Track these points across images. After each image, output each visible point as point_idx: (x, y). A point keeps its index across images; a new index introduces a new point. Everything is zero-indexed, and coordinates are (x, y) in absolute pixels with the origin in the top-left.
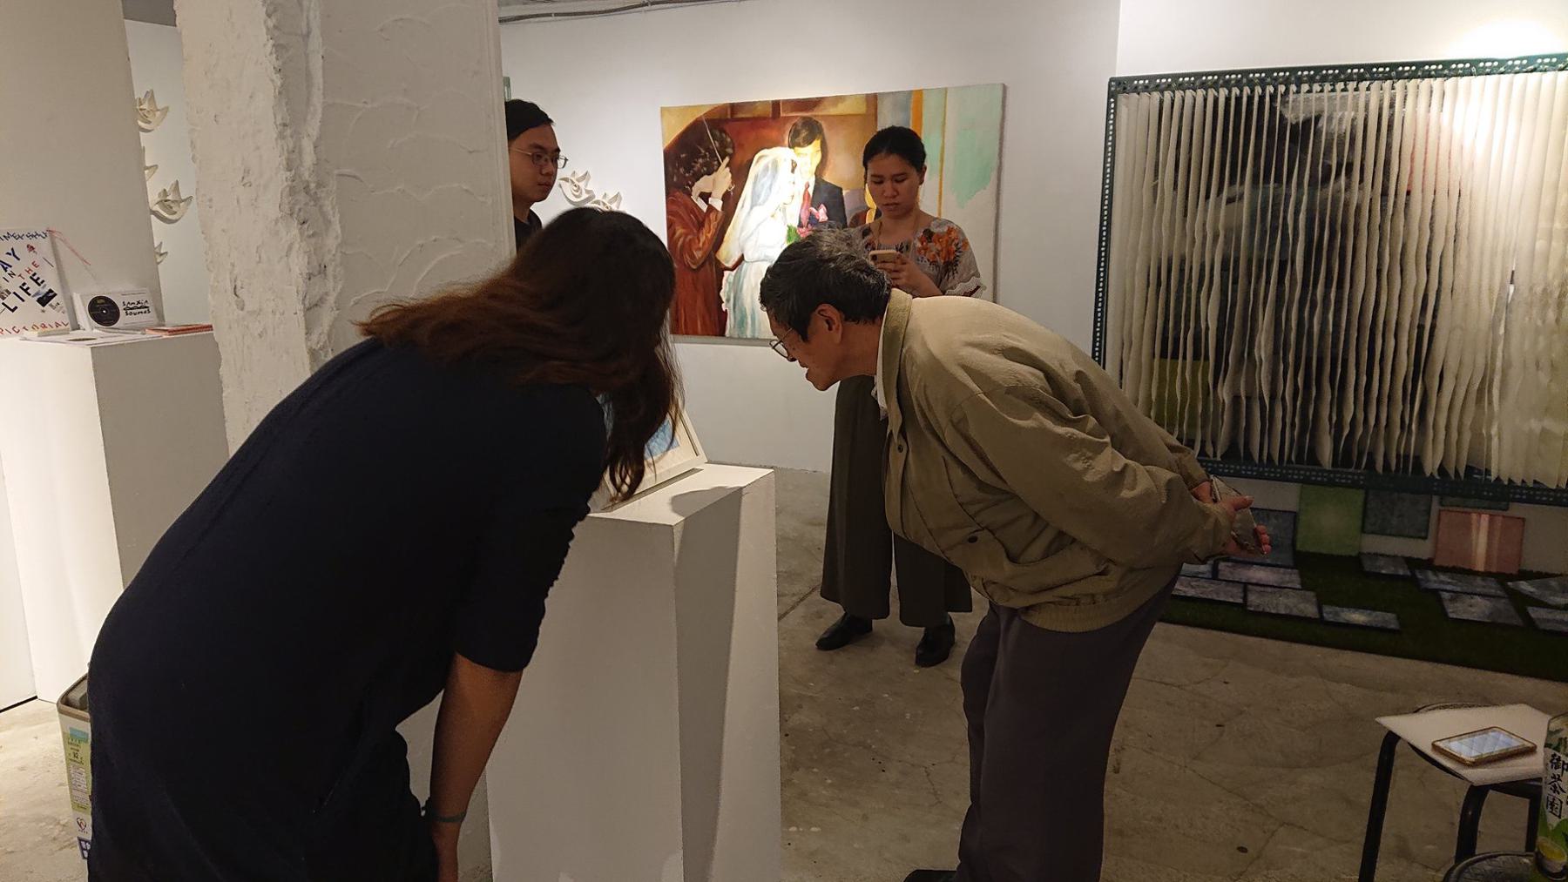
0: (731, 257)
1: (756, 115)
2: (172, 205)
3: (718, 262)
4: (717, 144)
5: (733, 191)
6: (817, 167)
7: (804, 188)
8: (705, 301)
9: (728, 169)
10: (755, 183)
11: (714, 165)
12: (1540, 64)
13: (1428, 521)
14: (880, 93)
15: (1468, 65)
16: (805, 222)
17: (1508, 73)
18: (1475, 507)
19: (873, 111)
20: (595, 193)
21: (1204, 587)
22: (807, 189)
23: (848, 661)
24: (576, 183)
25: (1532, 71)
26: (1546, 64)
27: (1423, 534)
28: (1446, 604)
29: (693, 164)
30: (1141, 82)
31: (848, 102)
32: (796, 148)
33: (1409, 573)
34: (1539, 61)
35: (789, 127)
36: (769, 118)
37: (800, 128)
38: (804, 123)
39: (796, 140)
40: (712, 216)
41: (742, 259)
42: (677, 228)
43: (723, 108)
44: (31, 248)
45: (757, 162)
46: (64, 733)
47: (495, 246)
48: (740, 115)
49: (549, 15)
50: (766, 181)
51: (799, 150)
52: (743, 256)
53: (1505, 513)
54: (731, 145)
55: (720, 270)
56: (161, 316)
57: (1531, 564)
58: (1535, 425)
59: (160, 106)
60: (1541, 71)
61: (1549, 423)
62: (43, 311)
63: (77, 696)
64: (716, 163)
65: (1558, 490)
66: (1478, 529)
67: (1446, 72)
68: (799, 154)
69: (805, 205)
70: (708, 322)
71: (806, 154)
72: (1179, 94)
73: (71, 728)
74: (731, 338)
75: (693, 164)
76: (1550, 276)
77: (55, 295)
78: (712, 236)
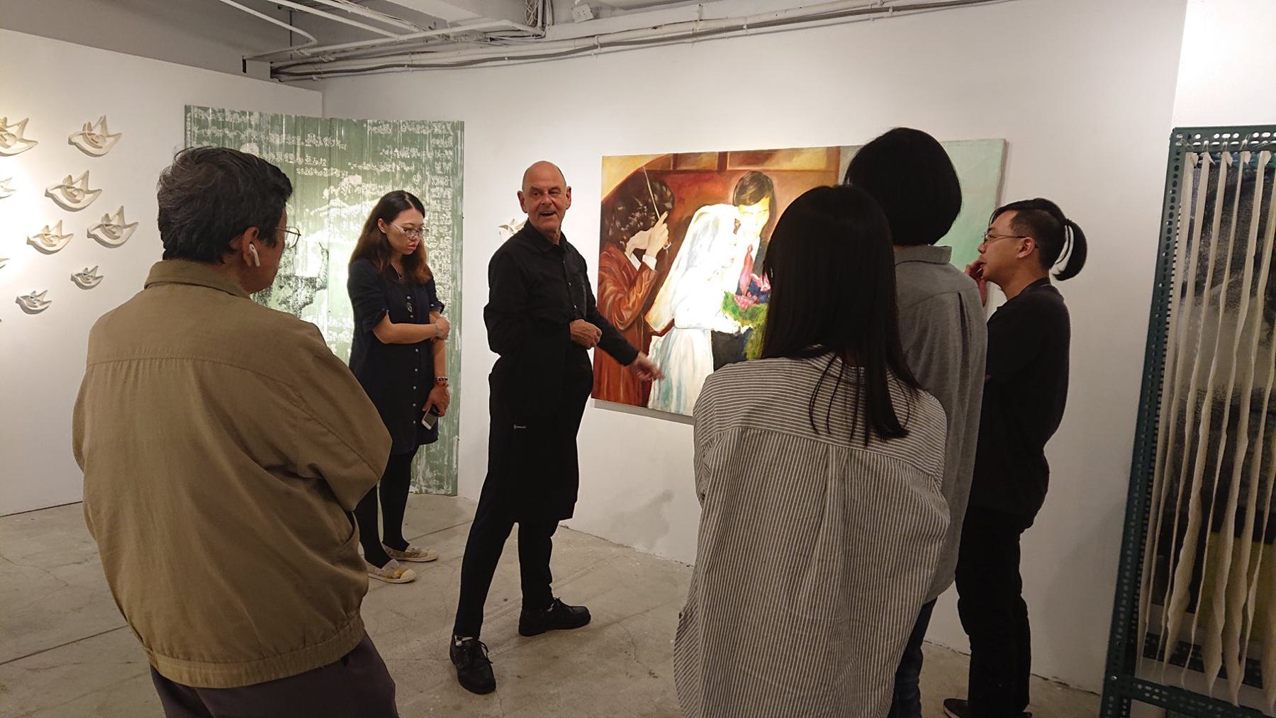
3: (647, 325)
4: (656, 198)
5: (669, 249)
9: (665, 225)
10: (692, 243)
11: (651, 220)
14: (844, 147)
16: (744, 289)
19: (833, 169)
29: (630, 218)
32: (742, 206)
35: (735, 182)
38: (752, 178)
39: (743, 197)
40: (645, 274)
41: (671, 324)
42: (608, 285)
43: (666, 158)
45: (697, 218)
48: (683, 168)
49: (503, 59)
52: (673, 320)
55: (649, 334)
64: (654, 217)
69: (746, 271)
70: (631, 391)
74: (654, 409)
78: (643, 297)
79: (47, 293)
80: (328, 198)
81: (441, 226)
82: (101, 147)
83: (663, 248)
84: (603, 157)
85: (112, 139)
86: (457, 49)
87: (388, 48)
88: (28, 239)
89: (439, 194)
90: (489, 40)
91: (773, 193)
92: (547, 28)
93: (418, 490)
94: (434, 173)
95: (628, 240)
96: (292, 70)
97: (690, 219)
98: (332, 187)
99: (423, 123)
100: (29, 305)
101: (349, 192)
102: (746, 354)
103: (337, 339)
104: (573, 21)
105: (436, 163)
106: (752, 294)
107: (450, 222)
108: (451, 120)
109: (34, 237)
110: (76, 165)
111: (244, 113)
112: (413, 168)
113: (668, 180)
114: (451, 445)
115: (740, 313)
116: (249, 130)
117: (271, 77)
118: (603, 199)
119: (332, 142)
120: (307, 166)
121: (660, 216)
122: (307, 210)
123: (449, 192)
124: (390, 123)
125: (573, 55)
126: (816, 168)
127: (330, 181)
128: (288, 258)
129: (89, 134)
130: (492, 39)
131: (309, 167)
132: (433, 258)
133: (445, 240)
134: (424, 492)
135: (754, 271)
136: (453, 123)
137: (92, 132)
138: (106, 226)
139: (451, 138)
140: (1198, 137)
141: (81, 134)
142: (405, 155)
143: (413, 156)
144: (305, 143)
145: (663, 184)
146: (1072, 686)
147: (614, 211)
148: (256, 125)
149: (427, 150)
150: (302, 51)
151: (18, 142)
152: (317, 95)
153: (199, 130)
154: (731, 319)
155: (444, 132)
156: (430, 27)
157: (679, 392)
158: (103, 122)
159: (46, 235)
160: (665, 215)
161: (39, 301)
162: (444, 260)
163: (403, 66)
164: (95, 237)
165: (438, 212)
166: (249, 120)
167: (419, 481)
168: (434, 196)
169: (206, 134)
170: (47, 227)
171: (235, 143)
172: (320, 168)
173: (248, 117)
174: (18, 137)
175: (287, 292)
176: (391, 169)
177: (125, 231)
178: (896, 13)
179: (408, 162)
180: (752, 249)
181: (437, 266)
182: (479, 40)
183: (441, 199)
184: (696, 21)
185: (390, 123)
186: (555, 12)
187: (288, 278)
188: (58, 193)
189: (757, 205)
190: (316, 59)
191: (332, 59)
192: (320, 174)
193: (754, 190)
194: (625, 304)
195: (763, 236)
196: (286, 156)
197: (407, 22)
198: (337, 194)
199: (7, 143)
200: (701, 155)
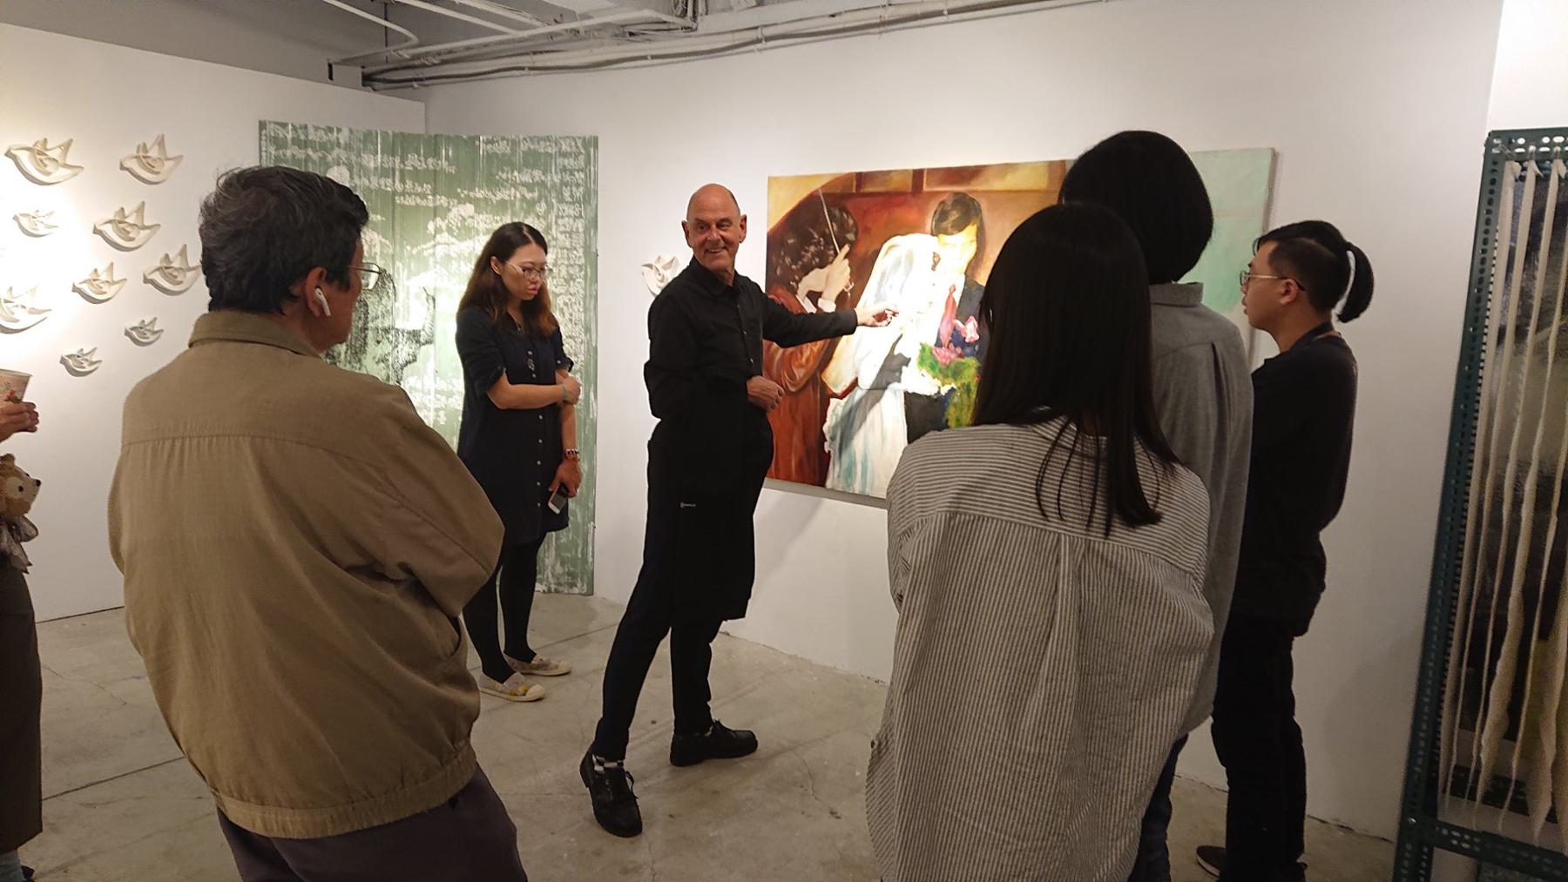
0: (841, 383)
3: (824, 386)
5: (851, 291)
6: (969, 265)
8: (804, 436)
9: (847, 261)
10: (880, 284)
11: (829, 256)
16: (945, 338)
22: (951, 293)
24: (662, 271)
29: (803, 253)
32: (942, 237)
35: (933, 206)
36: (909, 194)
39: (944, 224)
43: (848, 177)
45: (887, 252)
48: (869, 189)
49: (645, 58)
52: (856, 380)
54: (854, 229)
55: (826, 396)
59: (171, 152)
64: (832, 252)
68: (945, 244)
69: (948, 315)
74: (832, 490)
75: (803, 253)
79: (97, 351)
80: (433, 233)
81: (571, 265)
82: (157, 173)
83: (843, 290)
84: (769, 178)
85: (171, 163)
86: (589, 47)
87: (502, 47)
88: (74, 286)
89: (568, 226)
90: (628, 35)
91: (981, 220)
92: (699, 18)
93: (545, 588)
94: (561, 200)
95: (801, 279)
96: (387, 76)
97: (877, 253)
98: (438, 219)
99: (548, 139)
100: (75, 366)
101: (459, 225)
102: (947, 421)
103: (446, 406)
104: (731, 9)
105: (564, 188)
106: (955, 346)
107: (582, 261)
108: (582, 135)
109: (81, 283)
110: (129, 195)
111: (330, 130)
112: (536, 194)
113: (849, 205)
114: (586, 534)
115: (941, 371)
116: (337, 151)
117: (364, 85)
118: (769, 229)
119: (438, 164)
120: (408, 194)
121: (840, 249)
122: (409, 248)
123: (580, 225)
124: (507, 140)
125: (730, 52)
126: (1031, 189)
127: (436, 212)
128: (386, 307)
129: (144, 157)
130: (631, 34)
131: (410, 195)
132: (562, 306)
133: (576, 284)
134: (553, 590)
135: (957, 318)
136: (584, 139)
137: (148, 155)
138: (165, 268)
139: (582, 157)
140: (1521, 141)
141: (136, 157)
142: (526, 178)
143: (535, 181)
144: (405, 165)
145: (843, 209)
146: (1357, 831)
147: (783, 244)
148: (346, 144)
149: (553, 171)
150: (400, 52)
151: (60, 168)
152: (419, 106)
153: (276, 150)
154: (929, 377)
155: (574, 149)
156: (556, 21)
157: (864, 468)
158: (161, 143)
159: (95, 280)
160: (846, 248)
161: (87, 360)
162: (575, 308)
163: (523, 69)
164: (153, 282)
165: (567, 249)
166: (338, 139)
167: (547, 578)
168: (562, 229)
169: (285, 155)
170: (96, 270)
171: (320, 166)
172: (423, 196)
173: (335, 134)
174: (61, 161)
175: (385, 348)
176: (510, 196)
179: (530, 187)
180: (955, 290)
181: (567, 316)
182: (616, 35)
183: (570, 233)
184: (884, 6)
185: (507, 140)
187: (386, 331)
188: (109, 230)
189: (960, 233)
190: (417, 62)
191: (436, 62)
192: (424, 203)
193: (957, 216)
194: (797, 360)
195: (969, 273)
196: (382, 182)
197: (528, 15)
198: (444, 228)
199: (48, 169)
200: (892, 174)
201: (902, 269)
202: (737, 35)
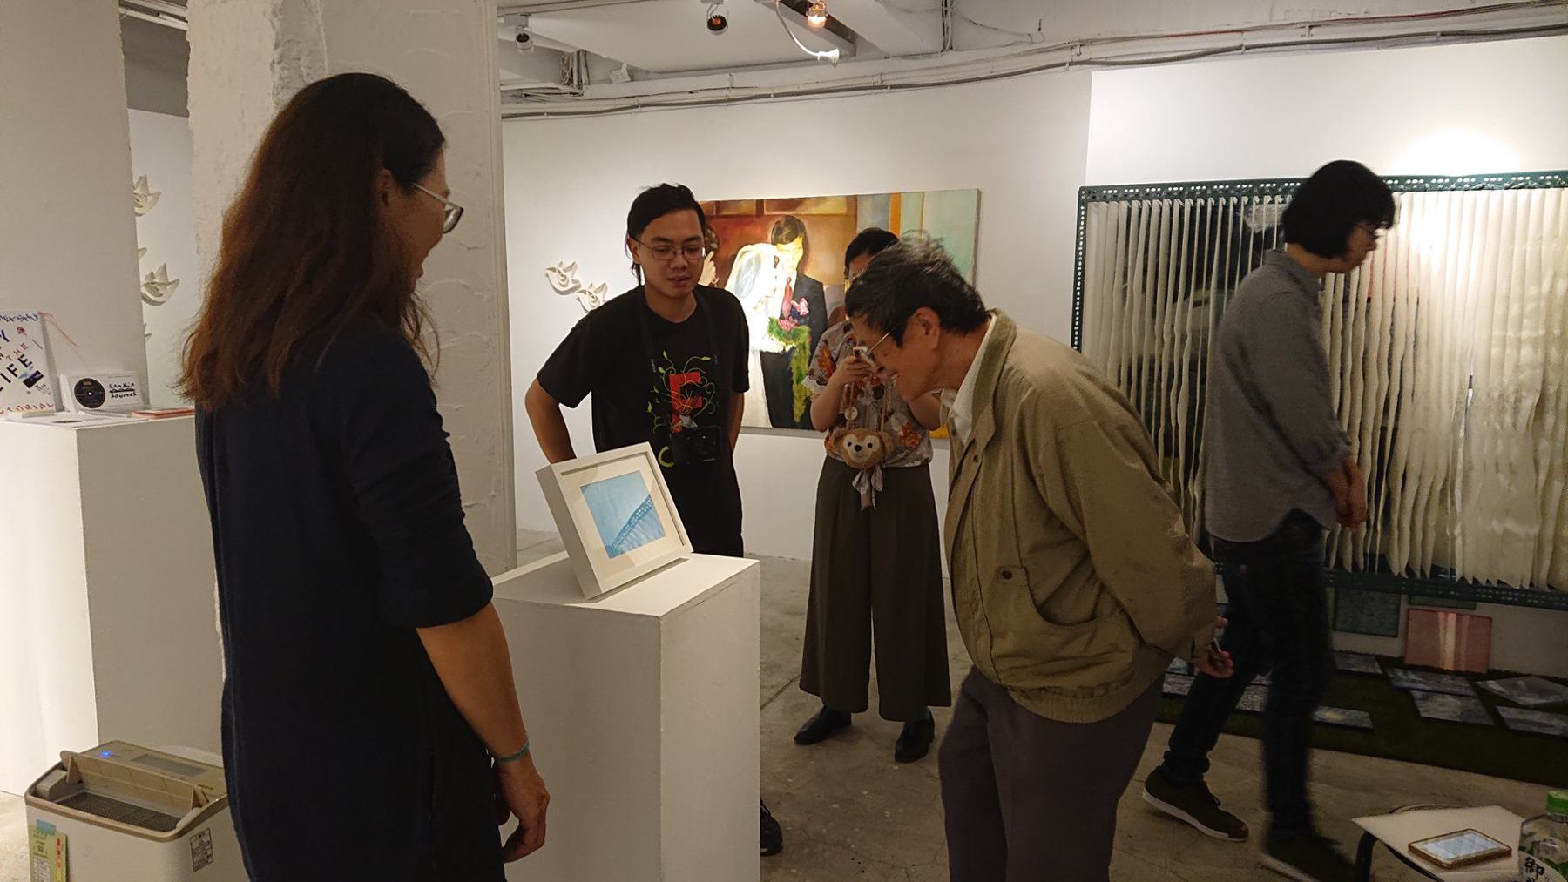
1: (740, 213)
2: (158, 287)
5: (717, 283)
7: (786, 283)
9: (712, 263)
10: (738, 277)
12: (1488, 183)
13: (1398, 619)
15: (1421, 181)
16: (786, 314)
17: (1459, 190)
18: (1442, 606)
19: (853, 213)
20: (581, 283)
21: (1180, 683)
22: (788, 283)
23: (827, 756)
24: (563, 273)
25: (1481, 189)
26: (1493, 183)
27: (1393, 633)
28: (1419, 703)
30: (1110, 192)
31: (828, 203)
32: (779, 245)
33: (1379, 671)
34: (1487, 179)
35: (772, 225)
37: (782, 226)
38: (787, 222)
39: (780, 237)
44: (21, 330)
45: (741, 256)
46: (30, 827)
47: (490, 339)
48: (726, 213)
49: (542, 114)
50: (749, 274)
51: (781, 246)
53: (1471, 612)
56: (146, 400)
57: (1499, 663)
58: (1497, 526)
59: (152, 190)
60: (1488, 189)
61: (1511, 525)
62: (29, 392)
63: (46, 786)
65: (1522, 590)
66: (1445, 628)
67: (1402, 187)
68: (781, 250)
71: (788, 251)
72: (1146, 203)
73: (38, 821)
76: (1506, 381)
77: (42, 376)
91: (805, 234)
92: (584, 87)
97: (735, 256)
102: (791, 369)
104: (611, 82)
106: (794, 318)
130: (526, 95)
135: (793, 299)
154: (776, 340)
160: (712, 254)
177: (168, 287)
178: (893, 90)
186: (591, 72)
189: (792, 243)
201: (753, 267)
202: (617, 102)
